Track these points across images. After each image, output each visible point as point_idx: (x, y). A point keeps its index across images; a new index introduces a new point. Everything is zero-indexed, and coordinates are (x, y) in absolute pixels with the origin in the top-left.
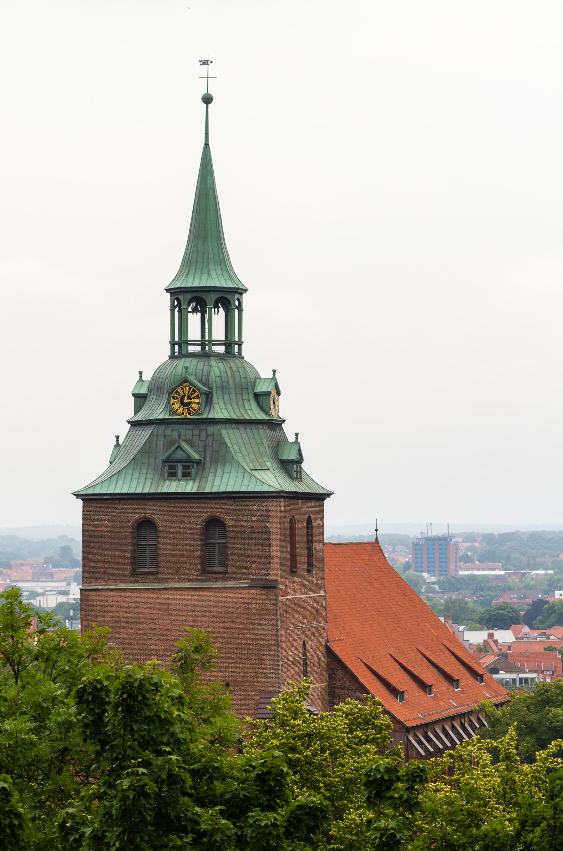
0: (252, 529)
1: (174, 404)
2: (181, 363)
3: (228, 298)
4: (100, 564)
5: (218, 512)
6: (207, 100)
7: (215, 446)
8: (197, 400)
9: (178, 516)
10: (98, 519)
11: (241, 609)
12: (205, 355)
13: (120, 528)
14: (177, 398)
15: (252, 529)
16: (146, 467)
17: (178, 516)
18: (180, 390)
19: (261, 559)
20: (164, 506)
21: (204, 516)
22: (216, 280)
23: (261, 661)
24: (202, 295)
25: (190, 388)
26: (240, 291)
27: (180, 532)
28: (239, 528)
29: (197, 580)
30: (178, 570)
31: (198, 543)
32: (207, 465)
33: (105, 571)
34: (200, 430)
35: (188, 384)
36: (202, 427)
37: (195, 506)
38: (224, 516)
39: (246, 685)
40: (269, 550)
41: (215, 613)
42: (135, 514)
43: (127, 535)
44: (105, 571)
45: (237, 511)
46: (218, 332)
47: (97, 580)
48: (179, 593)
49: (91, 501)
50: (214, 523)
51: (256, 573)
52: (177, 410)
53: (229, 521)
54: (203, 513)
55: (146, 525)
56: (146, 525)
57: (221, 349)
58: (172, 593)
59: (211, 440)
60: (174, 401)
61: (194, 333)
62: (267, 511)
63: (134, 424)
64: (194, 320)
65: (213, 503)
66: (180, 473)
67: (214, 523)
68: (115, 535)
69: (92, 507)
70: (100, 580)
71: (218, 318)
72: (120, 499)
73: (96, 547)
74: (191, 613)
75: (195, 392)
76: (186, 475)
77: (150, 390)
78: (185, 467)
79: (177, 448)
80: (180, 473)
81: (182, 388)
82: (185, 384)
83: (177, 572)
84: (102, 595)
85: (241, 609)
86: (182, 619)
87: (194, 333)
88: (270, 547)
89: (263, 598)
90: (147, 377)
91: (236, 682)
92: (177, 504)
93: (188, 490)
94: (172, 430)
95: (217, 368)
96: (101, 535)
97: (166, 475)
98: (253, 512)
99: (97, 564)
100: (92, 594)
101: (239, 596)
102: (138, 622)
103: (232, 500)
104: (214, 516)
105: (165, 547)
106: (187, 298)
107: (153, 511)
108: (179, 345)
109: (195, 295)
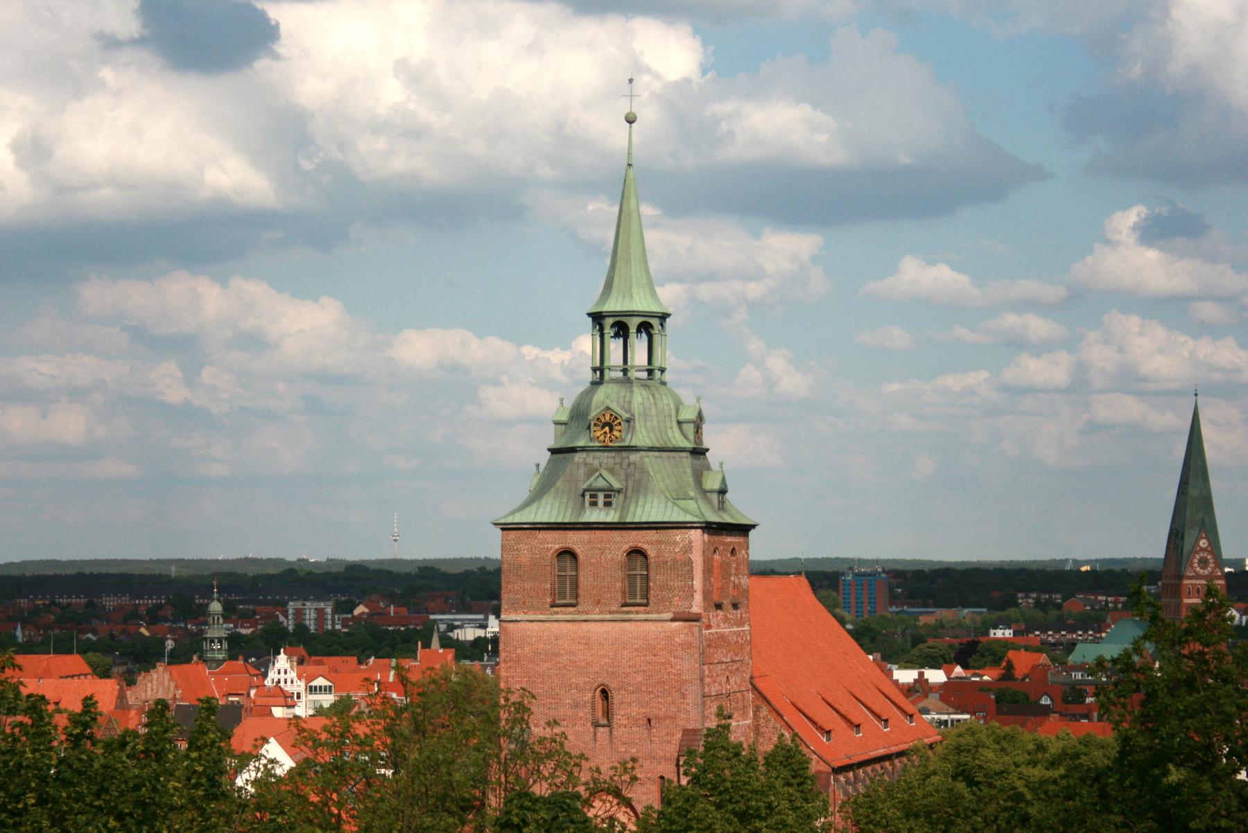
7: (637, 475)
15: (675, 561)
20: (585, 535)
21: (626, 547)
22: (640, 303)
23: (683, 696)
24: (624, 319)
26: (663, 317)
29: (618, 612)
30: (599, 602)
31: (619, 574)
32: (629, 494)
36: (624, 454)
37: (615, 534)
38: (645, 546)
39: (668, 722)
47: (516, 611)
48: (599, 624)
53: (651, 553)
57: (644, 375)
58: (593, 624)
62: (690, 542)
63: (553, 451)
65: (634, 533)
69: (512, 534)
72: (540, 529)
76: (608, 504)
77: (571, 418)
78: (606, 496)
86: (603, 652)
91: (657, 717)
93: (609, 519)
97: (587, 504)
98: (676, 543)
102: (557, 655)
105: (585, 579)
107: (573, 539)
109: (617, 319)
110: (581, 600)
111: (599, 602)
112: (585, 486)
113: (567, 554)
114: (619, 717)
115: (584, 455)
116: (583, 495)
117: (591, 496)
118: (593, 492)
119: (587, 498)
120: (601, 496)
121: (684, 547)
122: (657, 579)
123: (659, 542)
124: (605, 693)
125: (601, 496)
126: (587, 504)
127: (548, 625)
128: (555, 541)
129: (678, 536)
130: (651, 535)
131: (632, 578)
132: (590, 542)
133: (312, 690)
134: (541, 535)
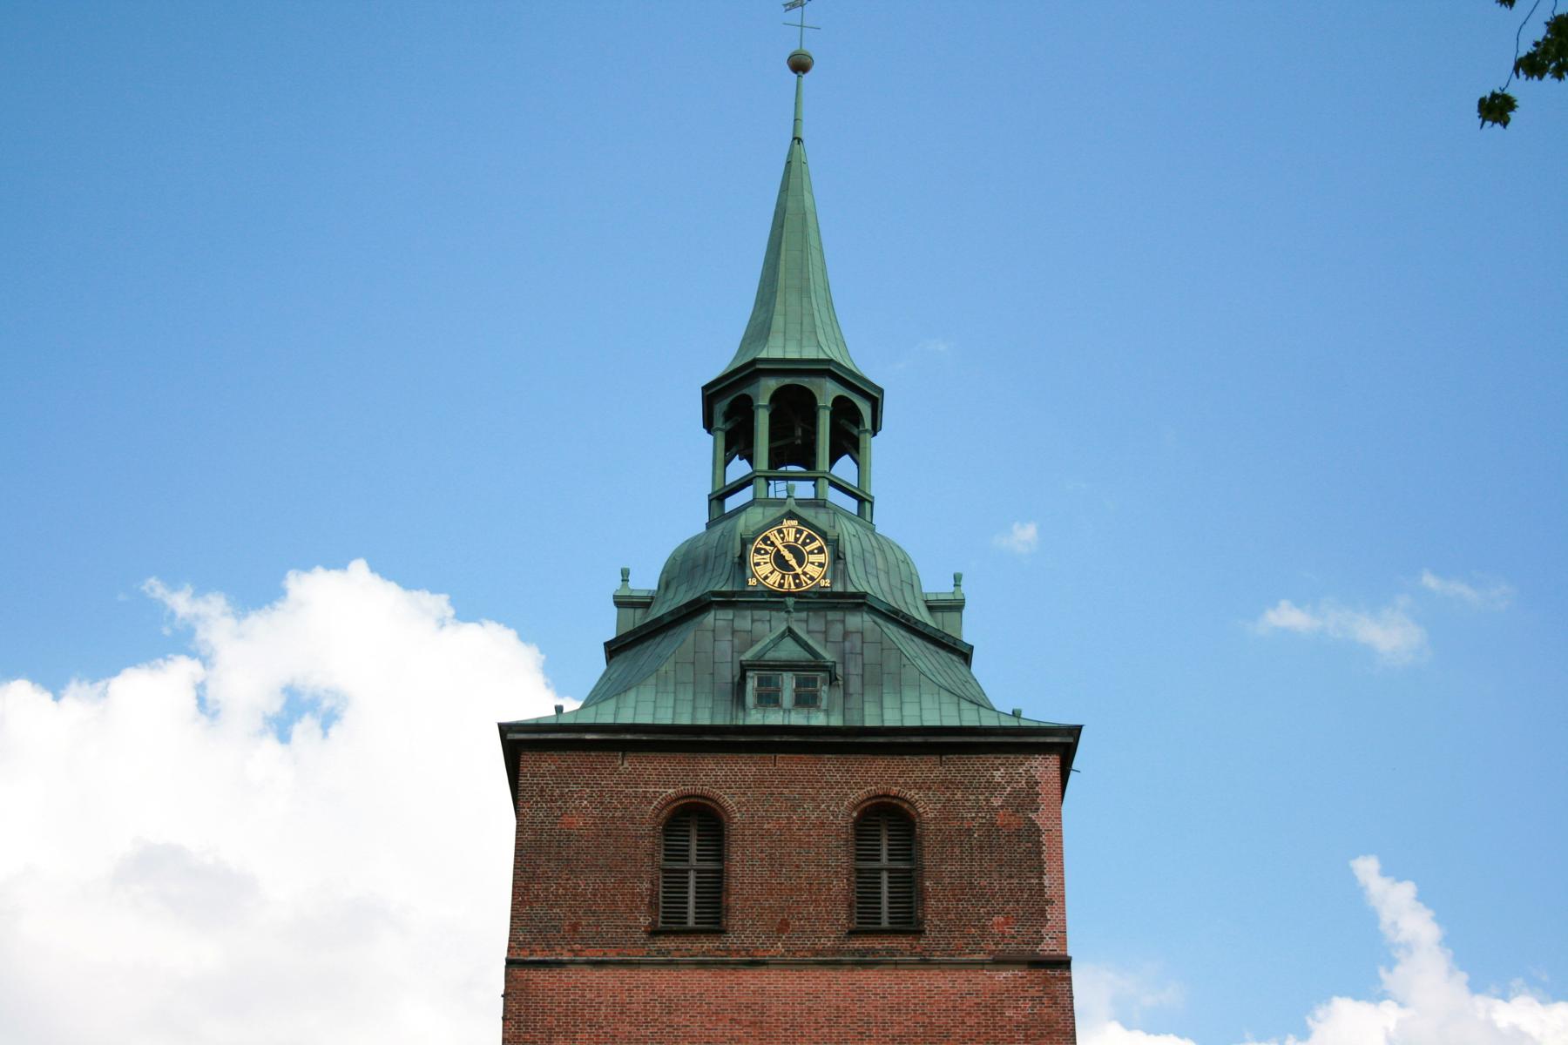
0: (991, 828)
1: (758, 564)
4: (560, 907)
5: (896, 784)
6: (800, 65)
7: (870, 654)
8: (821, 558)
9: (786, 791)
10: (562, 795)
11: (970, 1021)
13: (623, 817)
14: (767, 553)
15: (991, 828)
16: (690, 689)
17: (786, 791)
18: (773, 534)
19: (1018, 902)
20: (747, 767)
24: (805, 382)
25: (799, 532)
27: (791, 824)
28: (956, 824)
30: (784, 926)
31: (842, 859)
32: (855, 685)
33: (574, 927)
34: (827, 622)
35: (795, 523)
37: (831, 768)
38: (911, 794)
40: (1040, 878)
41: (896, 1030)
42: (665, 785)
43: (642, 837)
44: (574, 927)
45: (946, 784)
51: (1003, 937)
52: (766, 578)
53: (926, 807)
54: (849, 786)
59: (858, 643)
60: (757, 558)
62: (1033, 783)
66: (787, 696)
67: (885, 818)
68: (608, 835)
70: (558, 949)
73: (552, 864)
74: (826, 1030)
75: (813, 540)
76: (805, 700)
79: (782, 636)
80: (787, 696)
81: (780, 531)
82: (786, 523)
83: (781, 930)
84: (571, 976)
85: (970, 1021)
88: (1042, 873)
89: (1033, 992)
92: (786, 764)
94: (753, 621)
96: (569, 835)
98: (993, 787)
99: (551, 907)
100: (540, 976)
101: (966, 987)
103: (935, 759)
104: (885, 796)
105: (745, 868)
107: (714, 777)
109: (788, 381)
110: (734, 921)
111: (784, 926)
112: (748, 656)
113: (698, 819)
115: (728, 614)
116: (743, 678)
117: (762, 681)
118: (768, 669)
119: (752, 684)
120: (788, 682)
121: (1015, 794)
122: (941, 872)
123: (946, 784)
125: (788, 682)
126: (750, 698)
127: (645, 975)
128: (664, 781)
129: (999, 771)
130: (926, 768)
131: (865, 885)
132: (760, 782)
134: (626, 765)
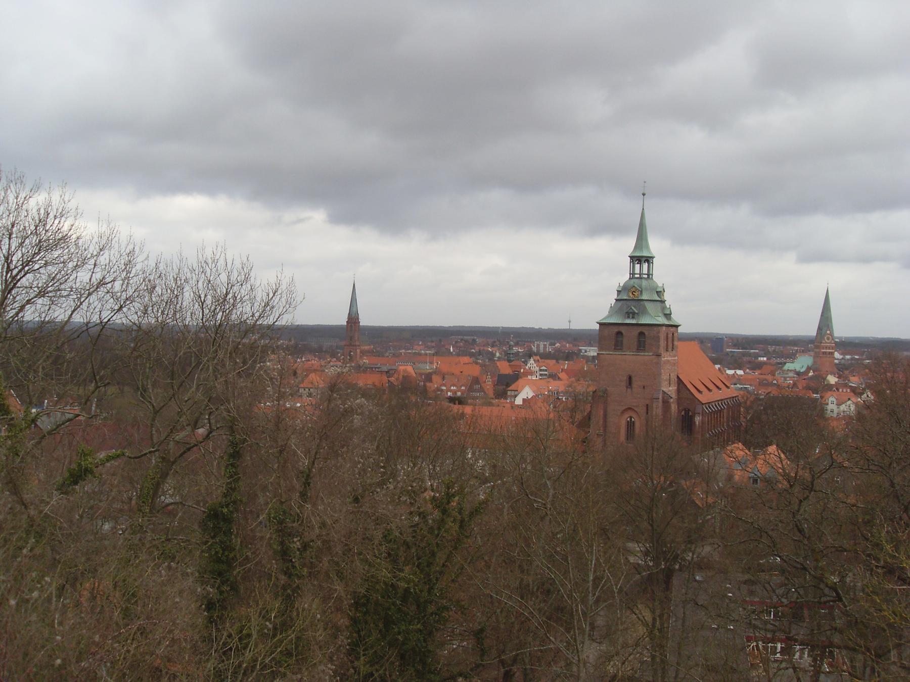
2: (633, 281)
3: (649, 260)
6: (644, 195)
12: (640, 278)
20: (625, 327)
22: (645, 254)
26: (653, 258)
46: (645, 271)
49: (601, 324)
50: (641, 334)
53: (646, 333)
55: (619, 334)
56: (619, 334)
61: (637, 270)
64: (637, 266)
67: (641, 334)
71: (645, 266)
76: (633, 318)
87: (637, 270)
90: (622, 285)
95: (644, 283)
105: (625, 342)
106: (636, 259)
108: (632, 274)
114: (634, 385)
124: (630, 378)
130: (646, 328)
131: (639, 342)
133: (541, 370)
